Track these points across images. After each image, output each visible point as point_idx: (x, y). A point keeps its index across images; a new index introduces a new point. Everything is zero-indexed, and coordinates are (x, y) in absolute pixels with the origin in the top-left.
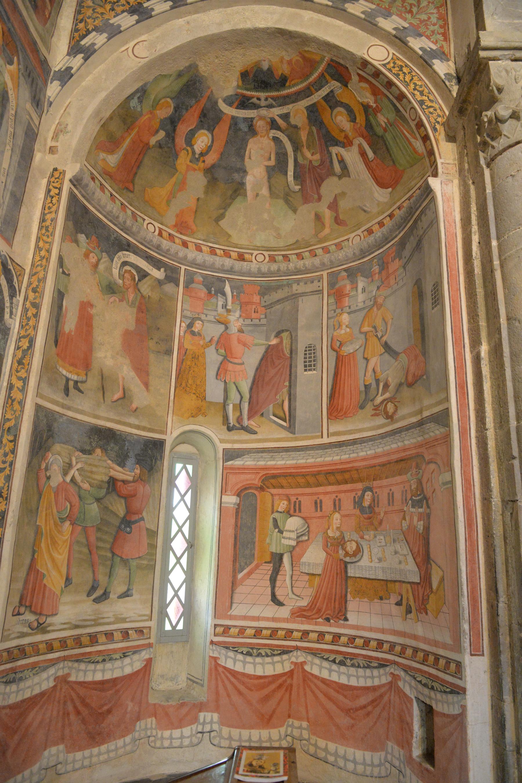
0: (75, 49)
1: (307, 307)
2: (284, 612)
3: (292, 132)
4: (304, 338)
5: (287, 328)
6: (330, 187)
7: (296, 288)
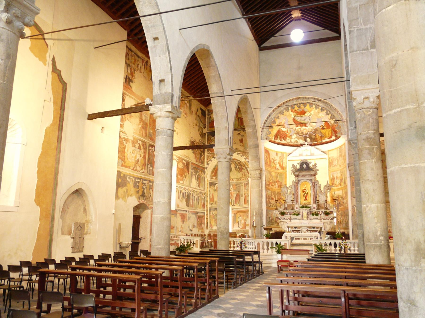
0: (208, 164)
1: (241, 188)
2: (240, 228)
3: (237, 164)
4: (241, 193)
5: (239, 191)
6: (243, 170)
7: (240, 185)
